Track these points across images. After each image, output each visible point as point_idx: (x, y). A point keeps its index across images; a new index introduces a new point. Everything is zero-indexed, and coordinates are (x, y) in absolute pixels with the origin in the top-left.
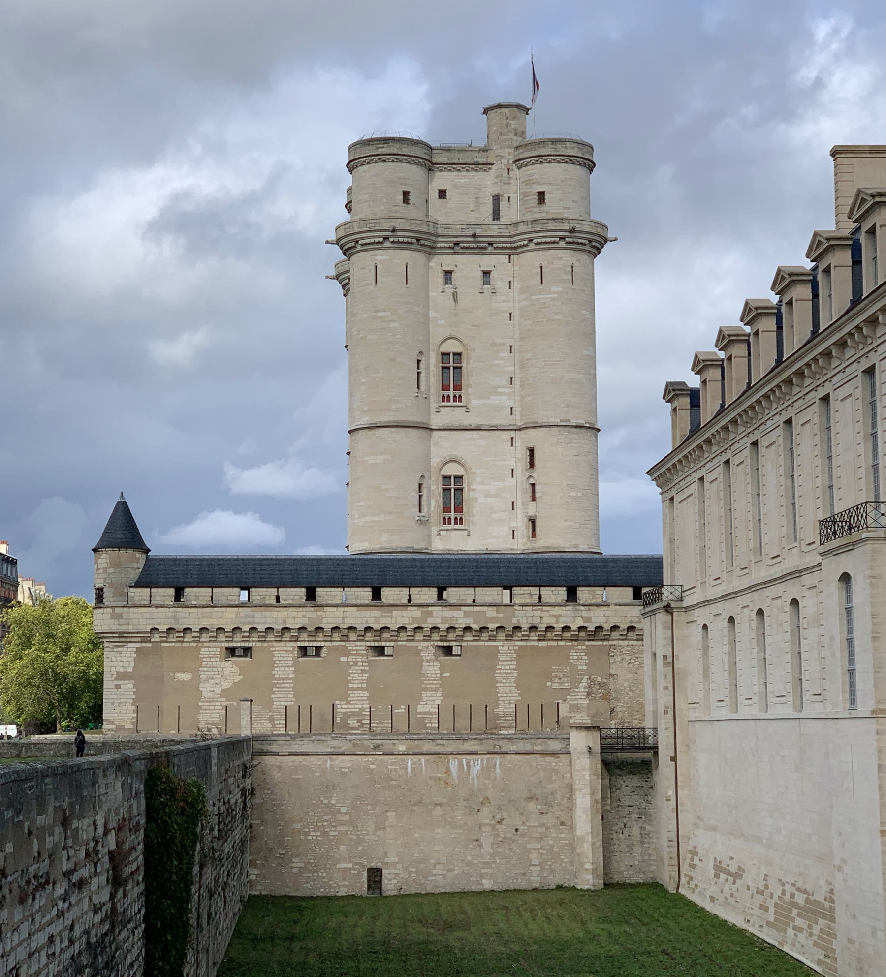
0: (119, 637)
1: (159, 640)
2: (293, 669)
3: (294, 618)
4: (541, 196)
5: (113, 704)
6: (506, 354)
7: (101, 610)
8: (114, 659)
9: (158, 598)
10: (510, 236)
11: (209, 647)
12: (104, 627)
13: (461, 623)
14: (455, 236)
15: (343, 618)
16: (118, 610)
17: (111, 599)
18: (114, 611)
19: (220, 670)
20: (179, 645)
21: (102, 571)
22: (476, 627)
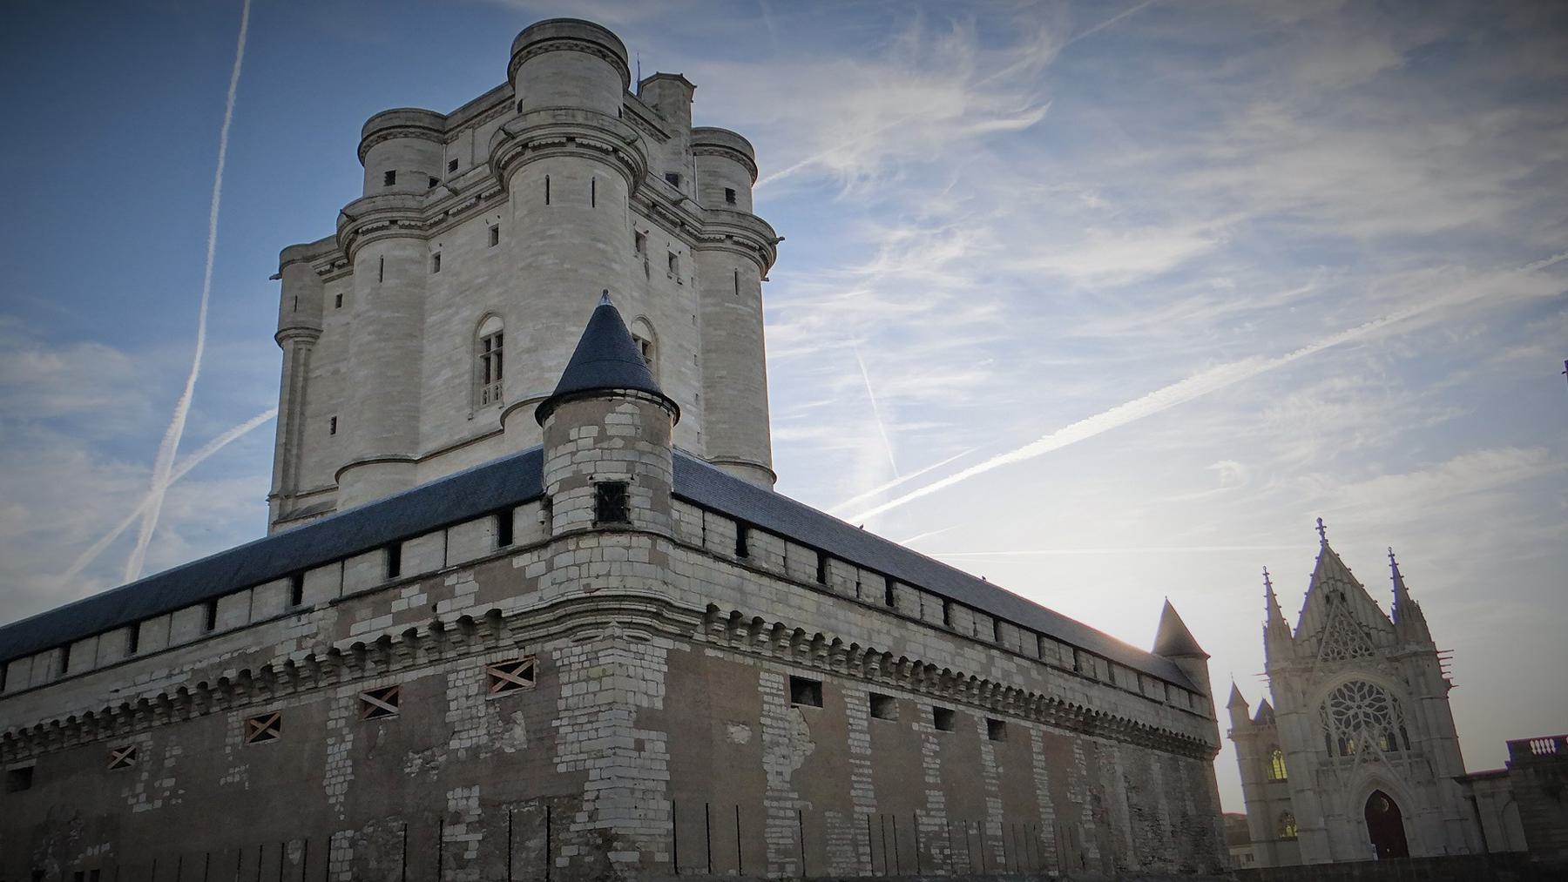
0: (657, 615)
1: (702, 638)
2: (868, 738)
3: (879, 632)
4: (730, 195)
5: (632, 791)
6: (690, 363)
7: (623, 539)
8: (631, 671)
9: (716, 539)
10: (703, 223)
11: (768, 671)
12: (630, 582)
13: (1018, 682)
14: (658, 193)
15: (925, 646)
16: (663, 546)
17: (648, 515)
18: (654, 545)
19: (787, 725)
20: (728, 657)
21: (619, 443)
22: (1026, 692)
